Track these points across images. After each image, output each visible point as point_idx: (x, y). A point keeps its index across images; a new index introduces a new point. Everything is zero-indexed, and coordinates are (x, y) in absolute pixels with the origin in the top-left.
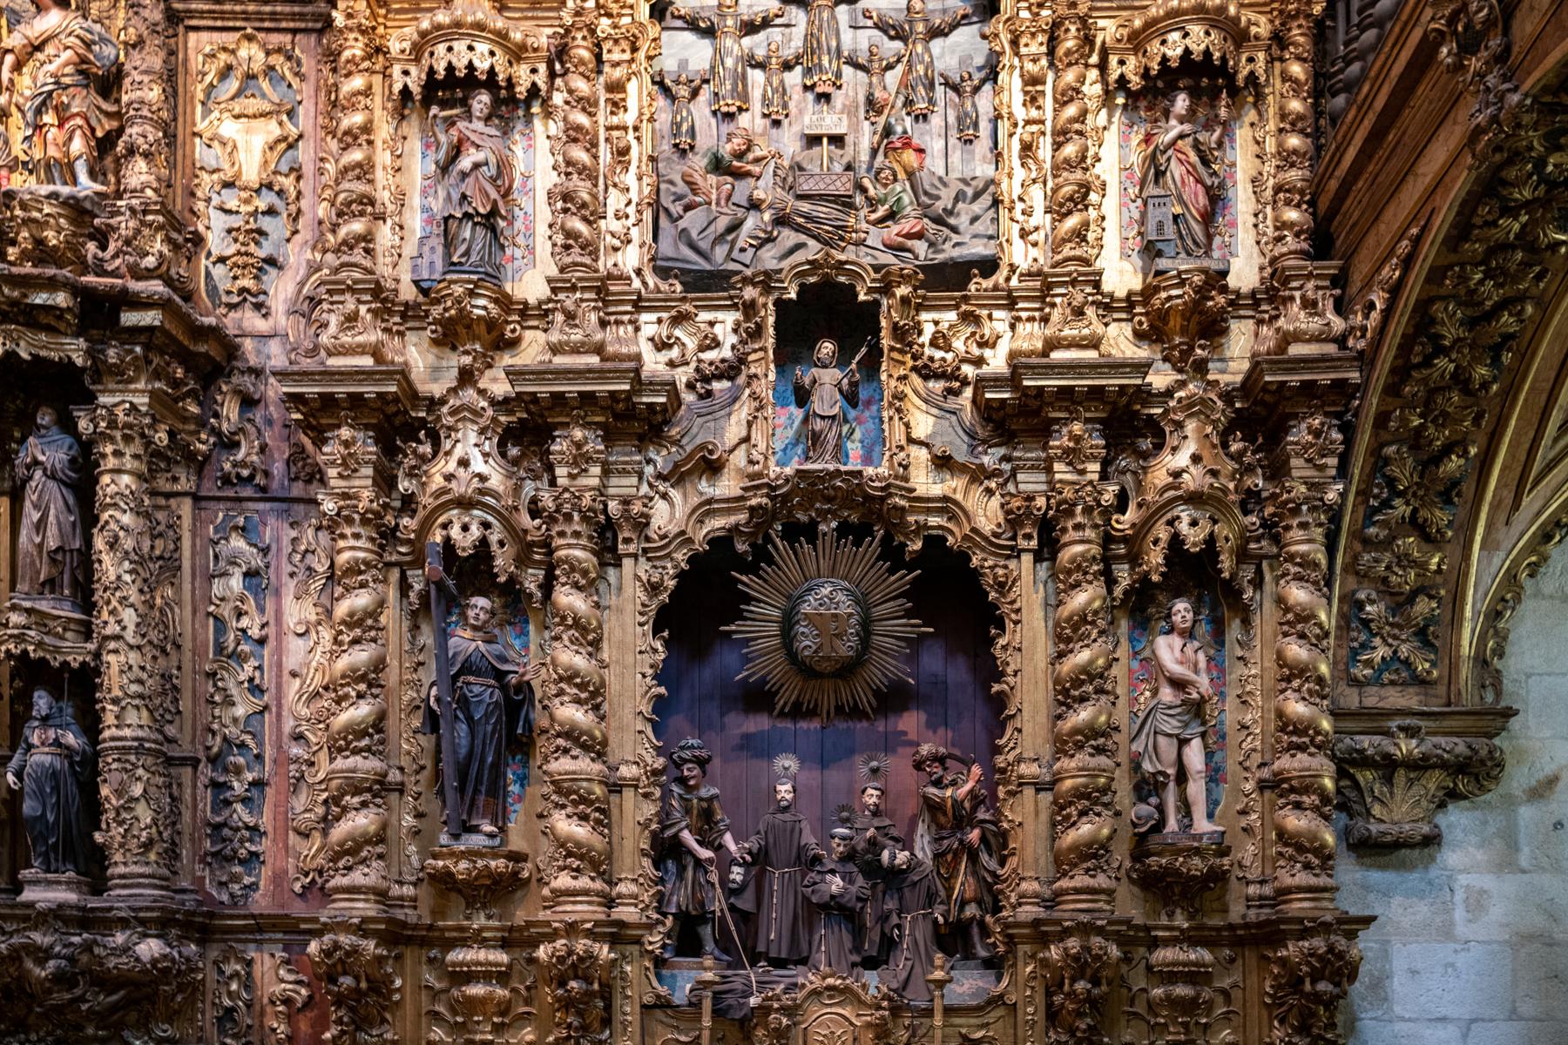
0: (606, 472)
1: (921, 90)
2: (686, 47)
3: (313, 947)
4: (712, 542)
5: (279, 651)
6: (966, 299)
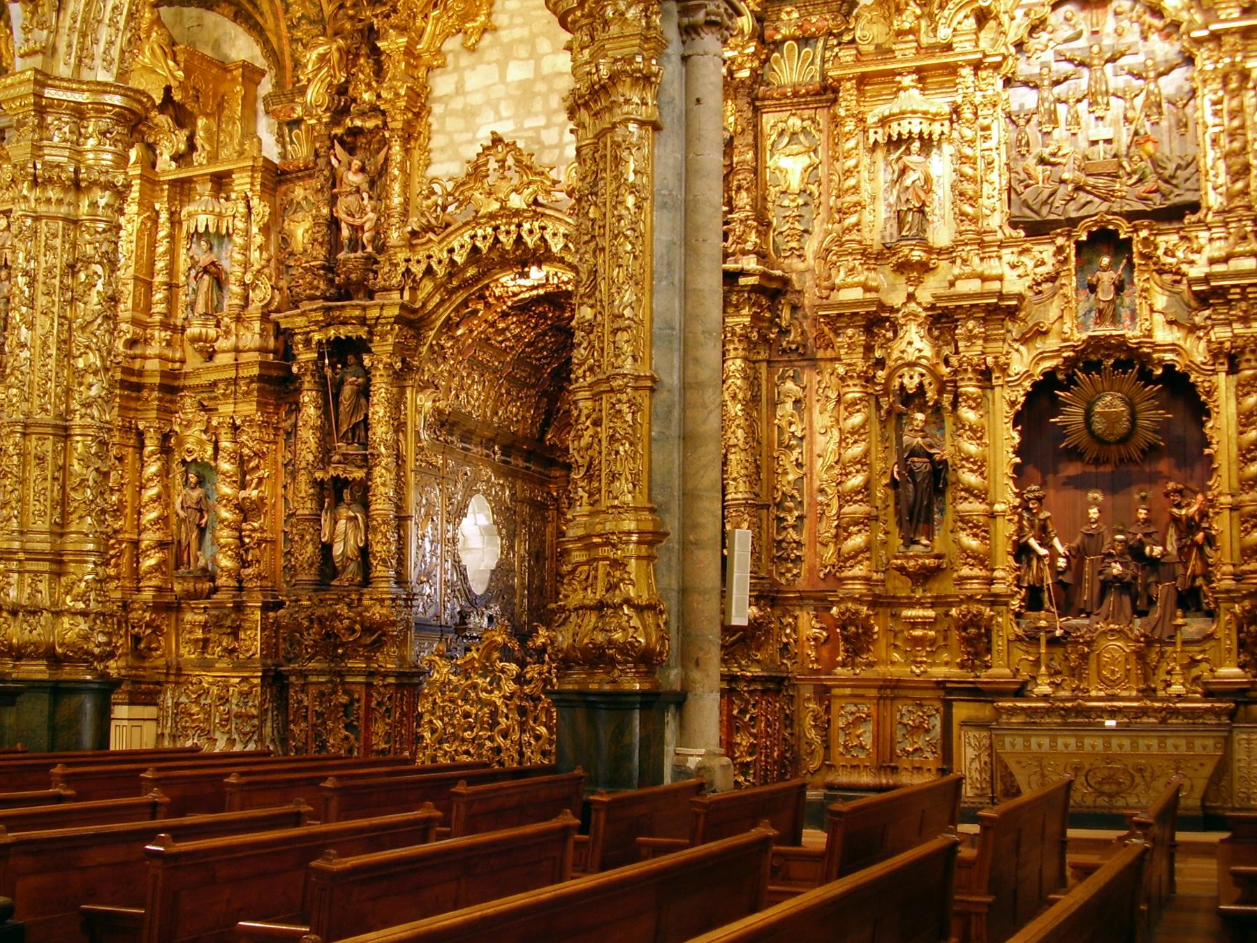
1: (1155, 110)
2: (1022, 96)
4: (1044, 374)
5: (811, 443)
6: (1181, 229)
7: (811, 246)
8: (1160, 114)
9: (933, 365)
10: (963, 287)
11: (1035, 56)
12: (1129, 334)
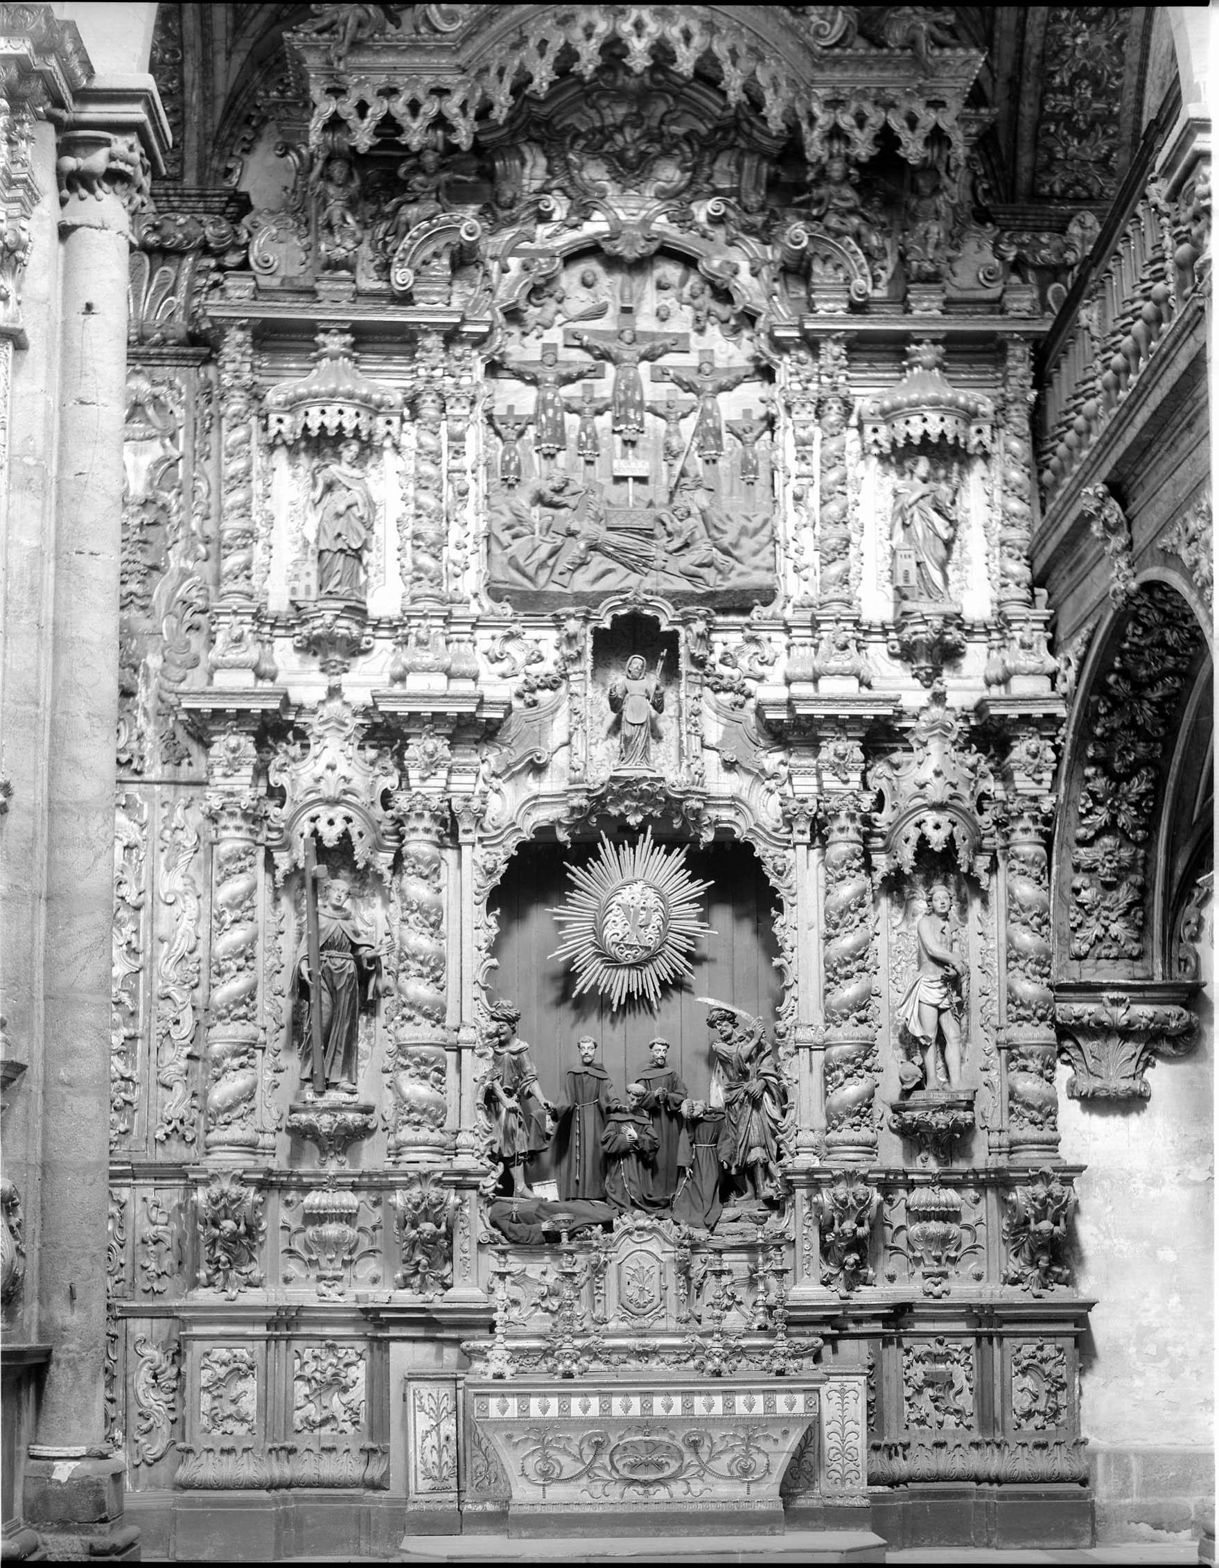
0: (450, 772)
4: (539, 831)
8: (719, 447)
11: (535, 333)
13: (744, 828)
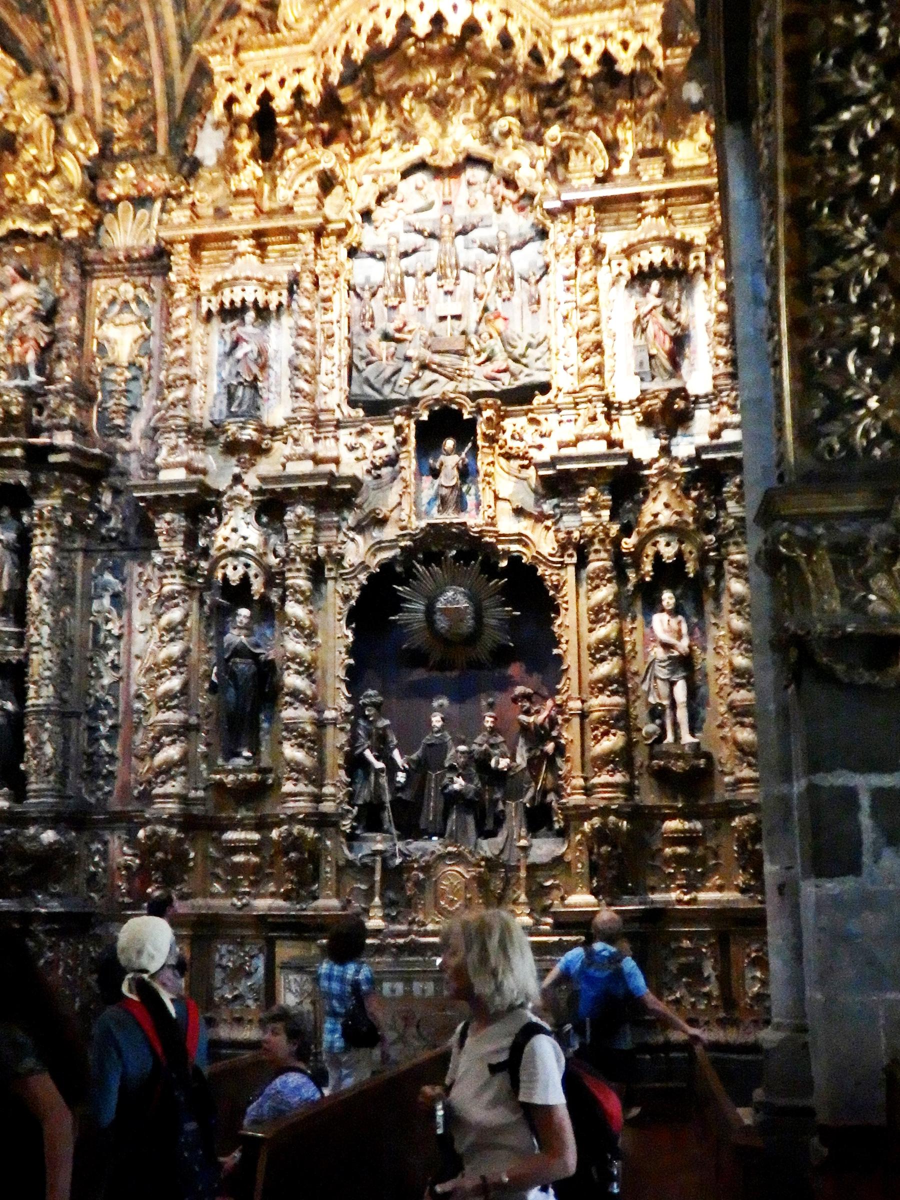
1: (506, 284)
3: (141, 834)
5: (129, 644)
6: (531, 411)
7: (138, 424)
9: (260, 555)
10: (295, 468)
12: (471, 522)
13: (529, 555)
